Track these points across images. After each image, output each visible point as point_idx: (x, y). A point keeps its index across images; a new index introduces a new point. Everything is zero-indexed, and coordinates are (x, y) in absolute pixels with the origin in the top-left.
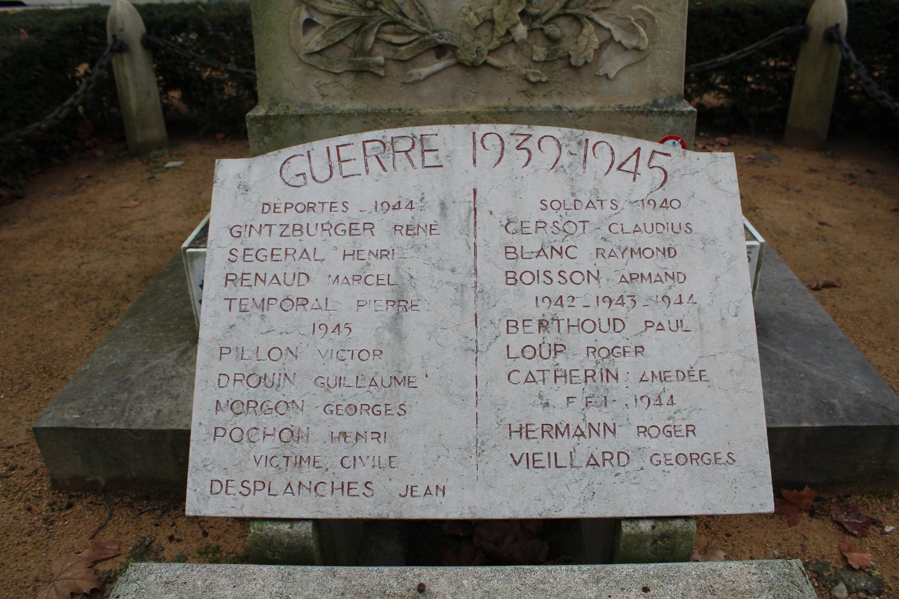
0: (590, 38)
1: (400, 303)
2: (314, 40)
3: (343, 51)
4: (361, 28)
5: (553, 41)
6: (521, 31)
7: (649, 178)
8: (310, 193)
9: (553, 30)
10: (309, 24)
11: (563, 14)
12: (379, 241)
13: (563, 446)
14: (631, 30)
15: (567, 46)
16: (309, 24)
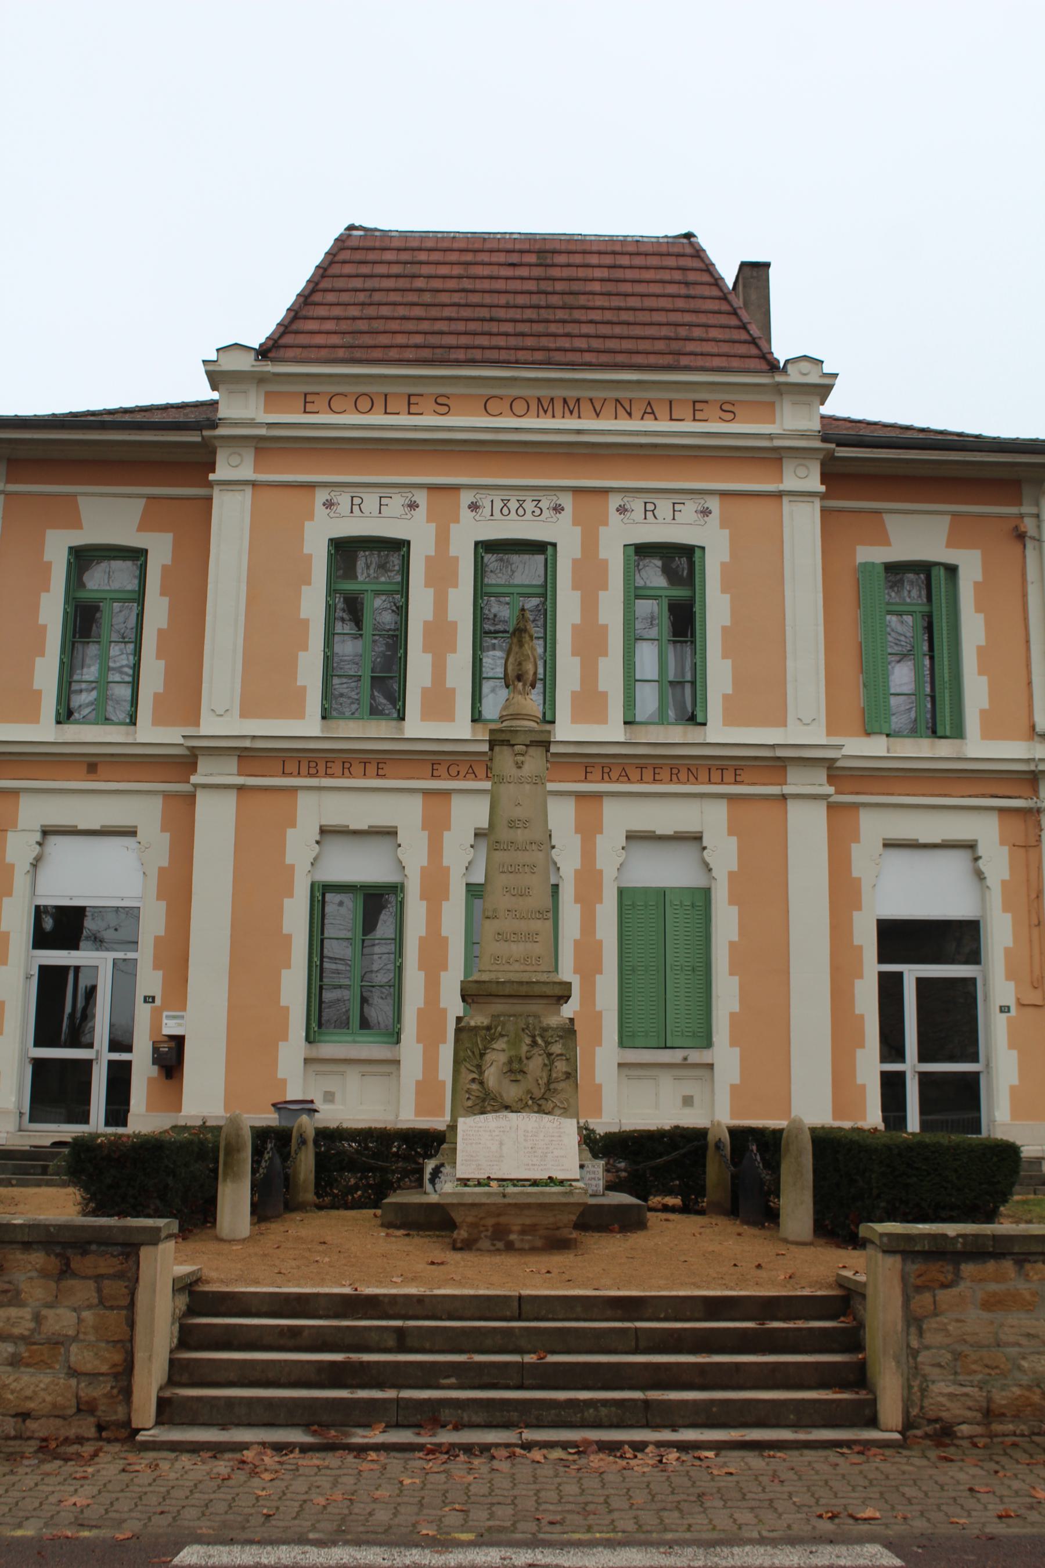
0: (550, 1105)
1: (501, 1144)
2: (470, 1103)
3: (478, 1107)
4: (484, 1100)
5: (540, 1105)
6: (530, 1102)
7: (556, 1123)
8: (480, 1124)
9: (540, 1102)
10: (468, 1098)
11: (542, 1098)
12: (497, 1133)
13: (536, 1168)
14: (562, 1102)
15: (543, 1107)
16: (468, 1098)
